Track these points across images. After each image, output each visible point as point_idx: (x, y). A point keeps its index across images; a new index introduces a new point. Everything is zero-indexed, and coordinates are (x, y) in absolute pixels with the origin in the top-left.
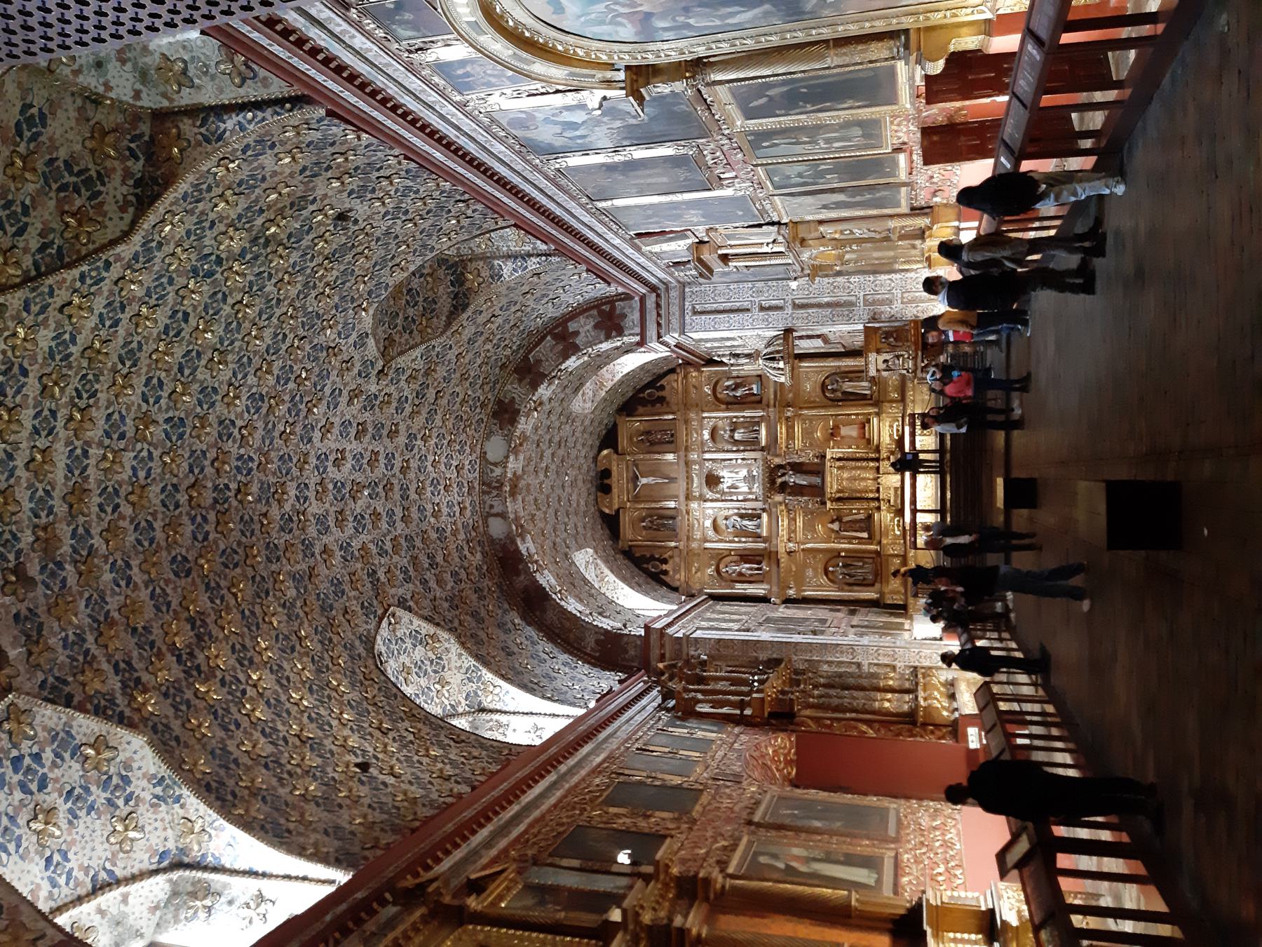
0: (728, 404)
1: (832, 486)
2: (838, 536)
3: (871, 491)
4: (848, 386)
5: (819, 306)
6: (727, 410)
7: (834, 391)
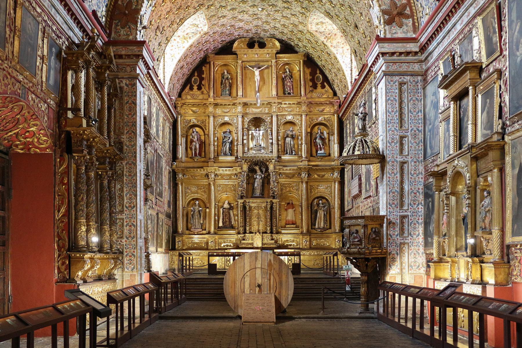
0: (311, 133)
1: (253, 203)
2: (218, 208)
3: (250, 229)
4: (321, 214)
5: (402, 182)
6: (307, 133)
7: (318, 204)
